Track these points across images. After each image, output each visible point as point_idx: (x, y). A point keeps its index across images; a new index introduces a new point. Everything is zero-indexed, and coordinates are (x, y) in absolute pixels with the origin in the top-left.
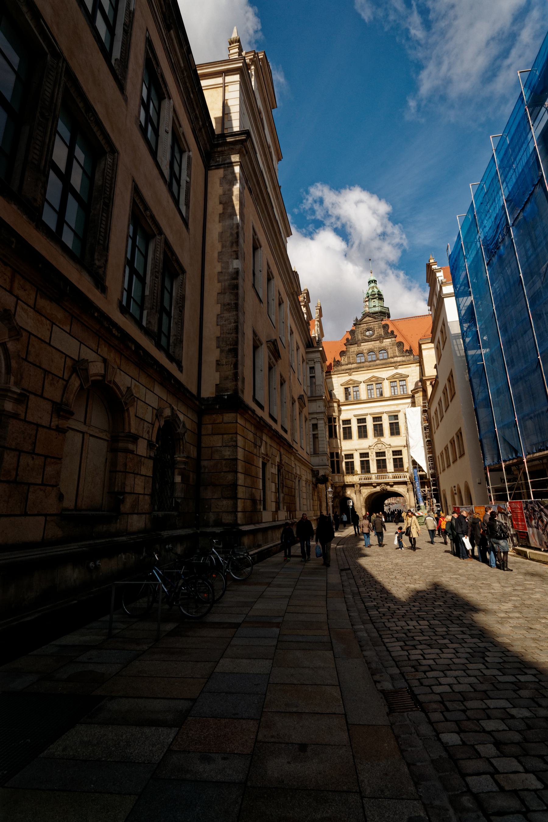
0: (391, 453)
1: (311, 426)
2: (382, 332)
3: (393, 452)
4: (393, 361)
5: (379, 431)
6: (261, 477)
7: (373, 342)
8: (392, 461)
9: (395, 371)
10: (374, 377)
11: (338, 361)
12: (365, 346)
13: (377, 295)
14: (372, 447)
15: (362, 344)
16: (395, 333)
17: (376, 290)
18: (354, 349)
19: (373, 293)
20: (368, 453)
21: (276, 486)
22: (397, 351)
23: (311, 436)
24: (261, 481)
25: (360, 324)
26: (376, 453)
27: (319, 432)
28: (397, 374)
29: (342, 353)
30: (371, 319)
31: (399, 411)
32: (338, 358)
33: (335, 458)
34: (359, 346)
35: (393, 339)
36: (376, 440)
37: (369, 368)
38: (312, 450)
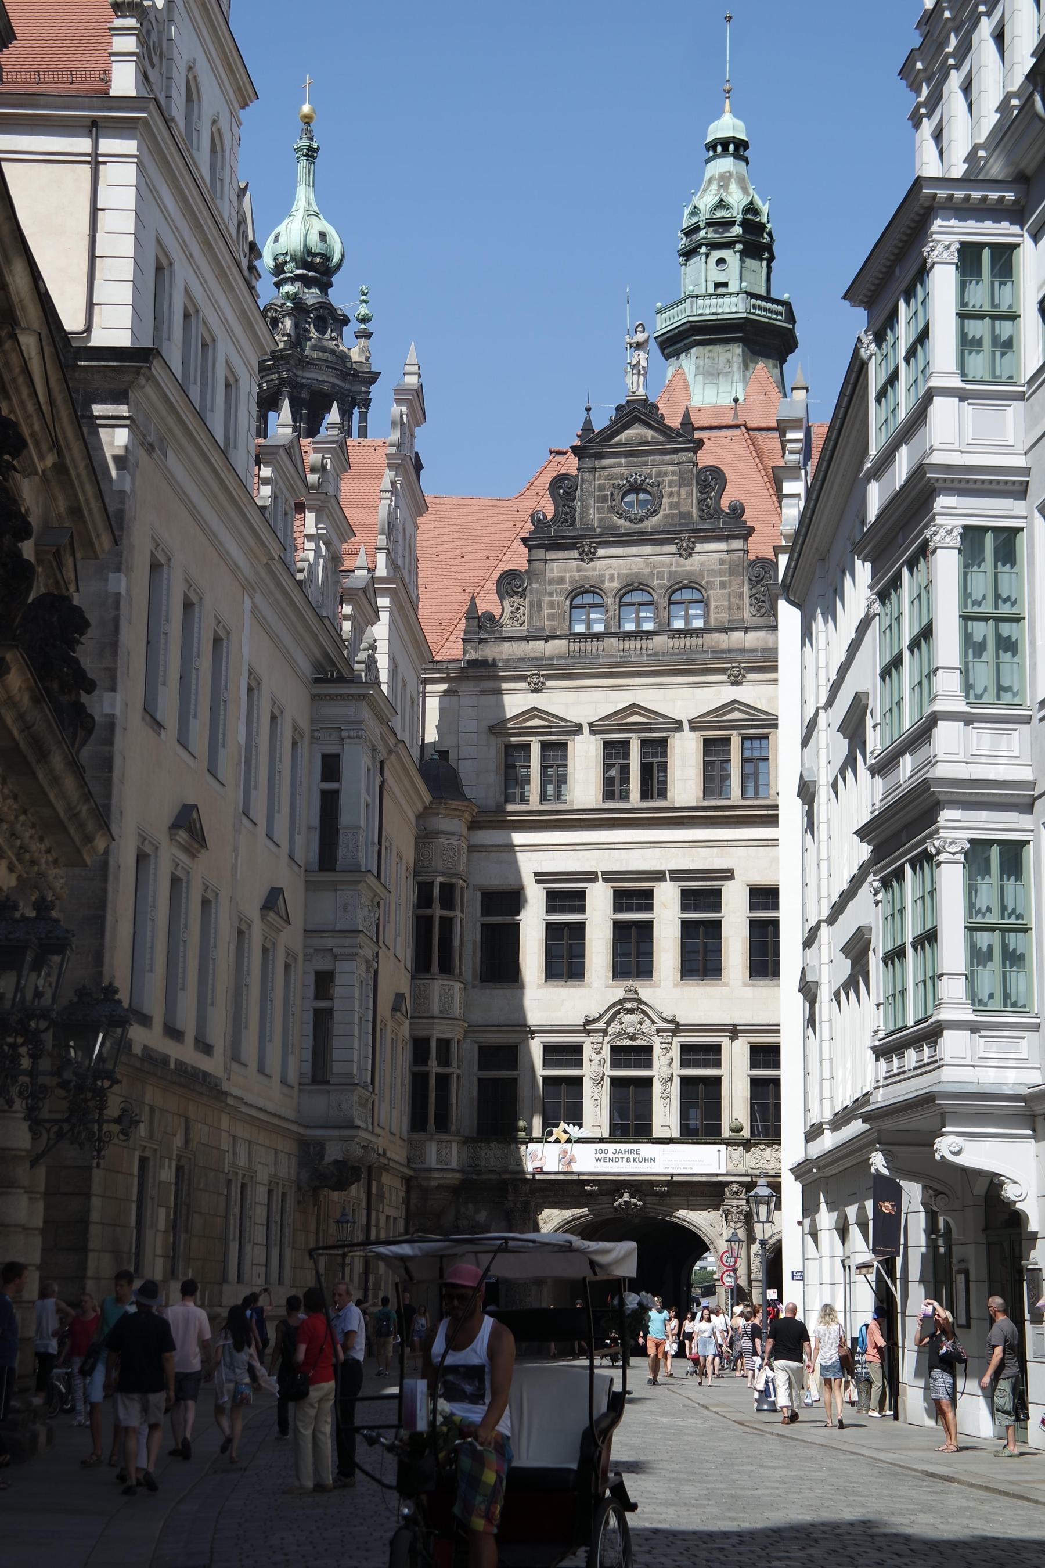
0: (675, 1052)
1: (311, 979)
2: (689, 500)
3: (685, 1048)
4: (724, 646)
5: (633, 953)
6: (135, 1198)
7: (648, 549)
8: (676, 1088)
9: (728, 693)
10: (633, 708)
11: (490, 617)
12: (614, 565)
13: (737, 230)
14: (601, 1025)
15: (601, 552)
16: (749, 518)
17: (737, 199)
18: (565, 568)
19: (720, 214)
20: (578, 1049)
21: (168, 1214)
22: (747, 600)
23: (310, 1017)
24: (134, 1206)
25: (600, 456)
26: (614, 1049)
27: (337, 1004)
28: (733, 705)
29: (510, 583)
30: (650, 434)
31: (728, 875)
32: (489, 602)
33: (433, 1062)
34: (589, 556)
35: (737, 544)
36: (618, 992)
37: (617, 671)
38: (307, 1068)
